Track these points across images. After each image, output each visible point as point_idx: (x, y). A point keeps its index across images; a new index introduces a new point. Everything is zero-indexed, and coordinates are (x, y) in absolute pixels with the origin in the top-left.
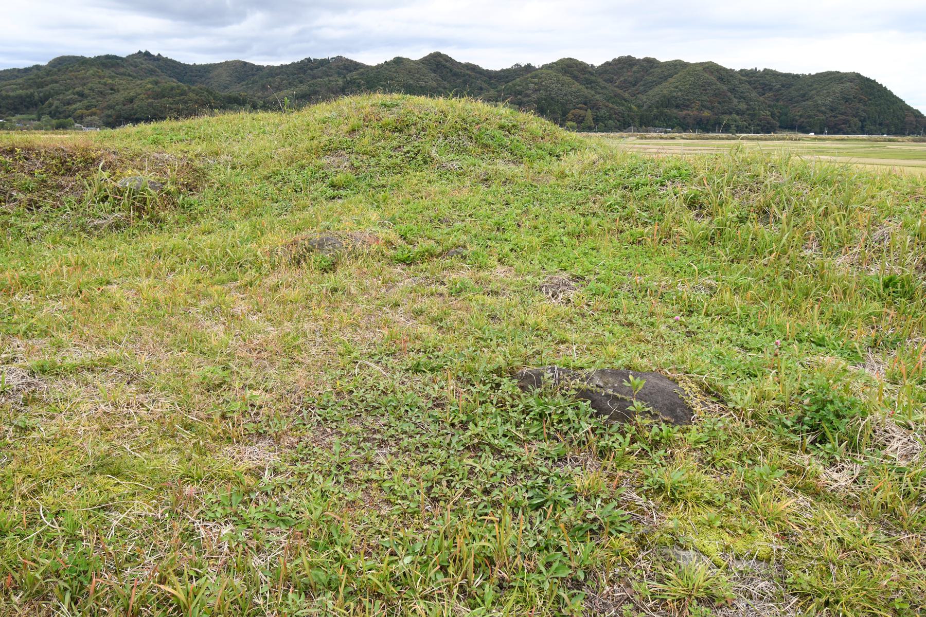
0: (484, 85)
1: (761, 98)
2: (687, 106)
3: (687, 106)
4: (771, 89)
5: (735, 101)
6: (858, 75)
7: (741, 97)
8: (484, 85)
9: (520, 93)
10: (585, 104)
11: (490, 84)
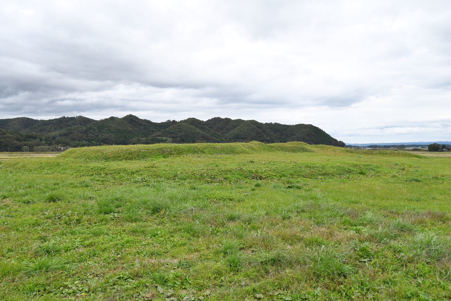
0: (154, 130)
1: (275, 135)
2: (246, 138)
3: (246, 138)
4: (278, 131)
5: (265, 136)
6: (312, 125)
7: (267, 135)
8: (154, 130)
9: (173, 133)
10: (202, 138)
11: (156, 129)
